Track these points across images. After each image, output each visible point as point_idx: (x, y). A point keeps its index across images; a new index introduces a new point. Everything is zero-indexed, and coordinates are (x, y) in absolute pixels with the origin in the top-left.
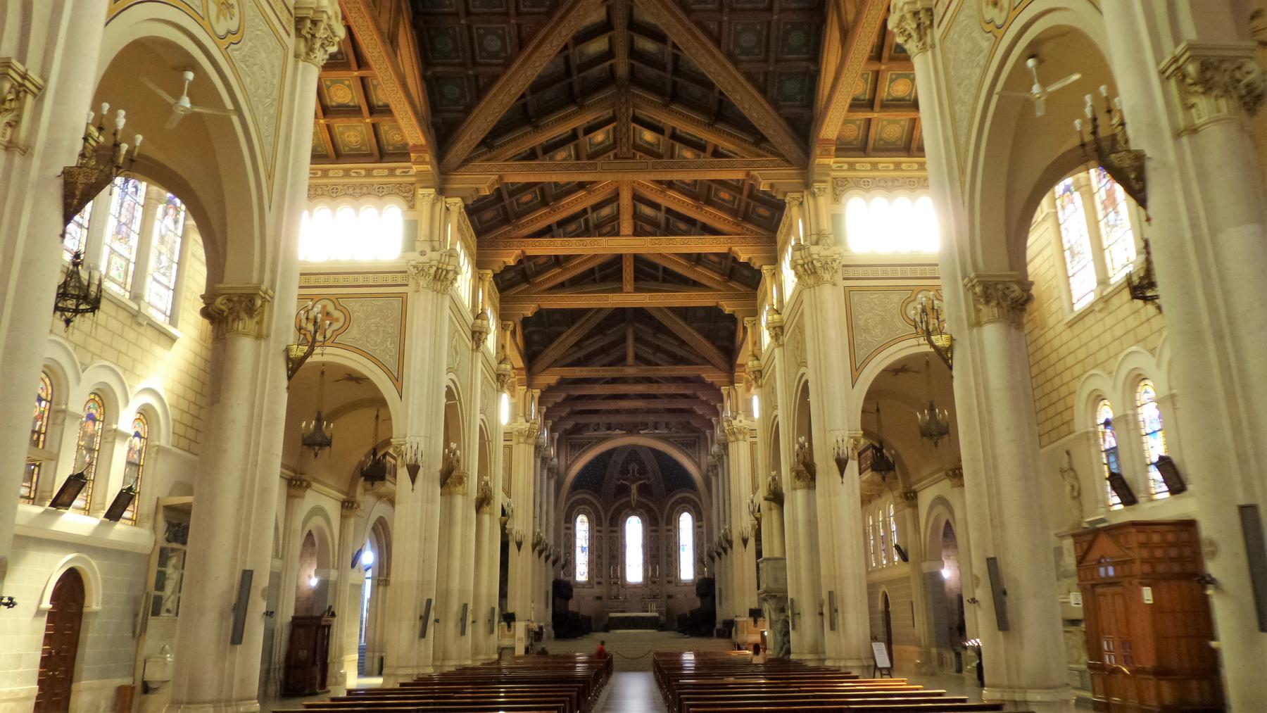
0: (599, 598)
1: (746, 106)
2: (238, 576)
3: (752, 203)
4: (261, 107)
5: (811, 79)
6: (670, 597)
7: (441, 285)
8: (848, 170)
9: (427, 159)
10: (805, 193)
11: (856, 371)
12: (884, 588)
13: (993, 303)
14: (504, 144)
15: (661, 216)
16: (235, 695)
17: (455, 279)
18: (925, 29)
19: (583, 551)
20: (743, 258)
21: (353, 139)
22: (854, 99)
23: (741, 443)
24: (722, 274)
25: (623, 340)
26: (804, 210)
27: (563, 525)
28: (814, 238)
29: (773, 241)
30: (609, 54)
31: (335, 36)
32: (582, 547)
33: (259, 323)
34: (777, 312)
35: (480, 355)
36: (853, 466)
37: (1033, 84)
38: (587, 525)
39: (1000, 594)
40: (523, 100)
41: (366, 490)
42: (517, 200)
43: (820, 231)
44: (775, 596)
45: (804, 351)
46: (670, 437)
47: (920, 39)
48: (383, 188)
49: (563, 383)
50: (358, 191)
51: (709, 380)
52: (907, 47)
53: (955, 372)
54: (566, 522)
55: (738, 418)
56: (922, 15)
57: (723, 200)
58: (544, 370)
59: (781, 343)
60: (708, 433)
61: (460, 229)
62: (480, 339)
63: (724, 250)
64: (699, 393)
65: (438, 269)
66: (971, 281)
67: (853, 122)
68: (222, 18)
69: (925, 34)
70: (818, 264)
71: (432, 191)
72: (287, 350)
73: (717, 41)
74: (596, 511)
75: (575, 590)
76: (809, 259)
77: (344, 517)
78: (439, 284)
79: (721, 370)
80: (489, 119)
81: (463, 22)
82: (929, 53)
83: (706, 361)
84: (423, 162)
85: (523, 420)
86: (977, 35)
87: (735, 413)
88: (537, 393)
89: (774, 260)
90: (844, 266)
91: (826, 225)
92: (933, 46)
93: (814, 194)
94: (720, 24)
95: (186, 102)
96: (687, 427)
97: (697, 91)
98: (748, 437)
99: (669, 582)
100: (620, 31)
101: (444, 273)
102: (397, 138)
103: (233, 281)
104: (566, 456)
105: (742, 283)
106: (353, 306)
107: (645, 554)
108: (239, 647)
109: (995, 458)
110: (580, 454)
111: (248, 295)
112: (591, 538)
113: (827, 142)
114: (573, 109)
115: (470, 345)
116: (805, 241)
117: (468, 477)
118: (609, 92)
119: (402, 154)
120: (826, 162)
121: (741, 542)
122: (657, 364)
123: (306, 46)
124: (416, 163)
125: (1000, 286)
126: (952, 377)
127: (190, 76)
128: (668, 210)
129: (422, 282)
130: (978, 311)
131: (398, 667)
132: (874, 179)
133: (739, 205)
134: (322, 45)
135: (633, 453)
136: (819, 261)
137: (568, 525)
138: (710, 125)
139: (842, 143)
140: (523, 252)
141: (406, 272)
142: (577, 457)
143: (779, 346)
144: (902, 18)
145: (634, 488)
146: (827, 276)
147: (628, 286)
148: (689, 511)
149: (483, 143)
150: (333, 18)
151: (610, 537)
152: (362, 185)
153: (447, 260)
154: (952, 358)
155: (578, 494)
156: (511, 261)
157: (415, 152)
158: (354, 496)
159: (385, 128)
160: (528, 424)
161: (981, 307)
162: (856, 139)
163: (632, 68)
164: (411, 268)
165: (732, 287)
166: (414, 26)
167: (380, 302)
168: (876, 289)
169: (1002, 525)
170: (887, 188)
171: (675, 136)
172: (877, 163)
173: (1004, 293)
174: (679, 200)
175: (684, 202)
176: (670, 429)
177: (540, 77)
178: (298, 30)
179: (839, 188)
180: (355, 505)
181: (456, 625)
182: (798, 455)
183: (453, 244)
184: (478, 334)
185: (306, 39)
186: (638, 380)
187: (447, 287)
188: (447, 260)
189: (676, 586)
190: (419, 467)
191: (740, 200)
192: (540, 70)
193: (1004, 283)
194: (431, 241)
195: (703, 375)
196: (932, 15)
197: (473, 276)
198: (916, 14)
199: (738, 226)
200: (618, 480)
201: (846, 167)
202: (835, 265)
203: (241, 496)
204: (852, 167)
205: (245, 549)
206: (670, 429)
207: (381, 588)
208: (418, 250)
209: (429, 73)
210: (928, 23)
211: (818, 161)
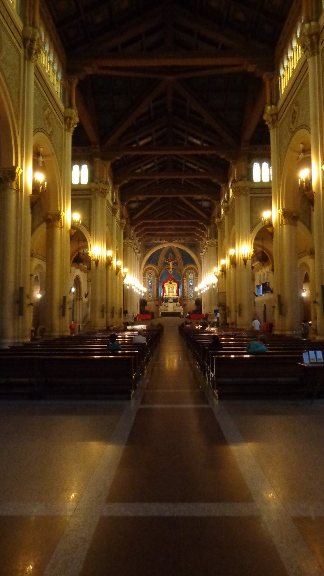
33: (61, 223)
34: (227, 202)
52: (269, 126)
54: (144, 276)
75: (147, 302)
89: (226, 182)
99: (185, 300)
110: (149, 250)
115: (112, 214)
134: (73, 126)
135: (170, 250)
137: (145, 278)
145: (171, 263)
164: (93, 189)
200: (165, 260)
210: (275, 119)
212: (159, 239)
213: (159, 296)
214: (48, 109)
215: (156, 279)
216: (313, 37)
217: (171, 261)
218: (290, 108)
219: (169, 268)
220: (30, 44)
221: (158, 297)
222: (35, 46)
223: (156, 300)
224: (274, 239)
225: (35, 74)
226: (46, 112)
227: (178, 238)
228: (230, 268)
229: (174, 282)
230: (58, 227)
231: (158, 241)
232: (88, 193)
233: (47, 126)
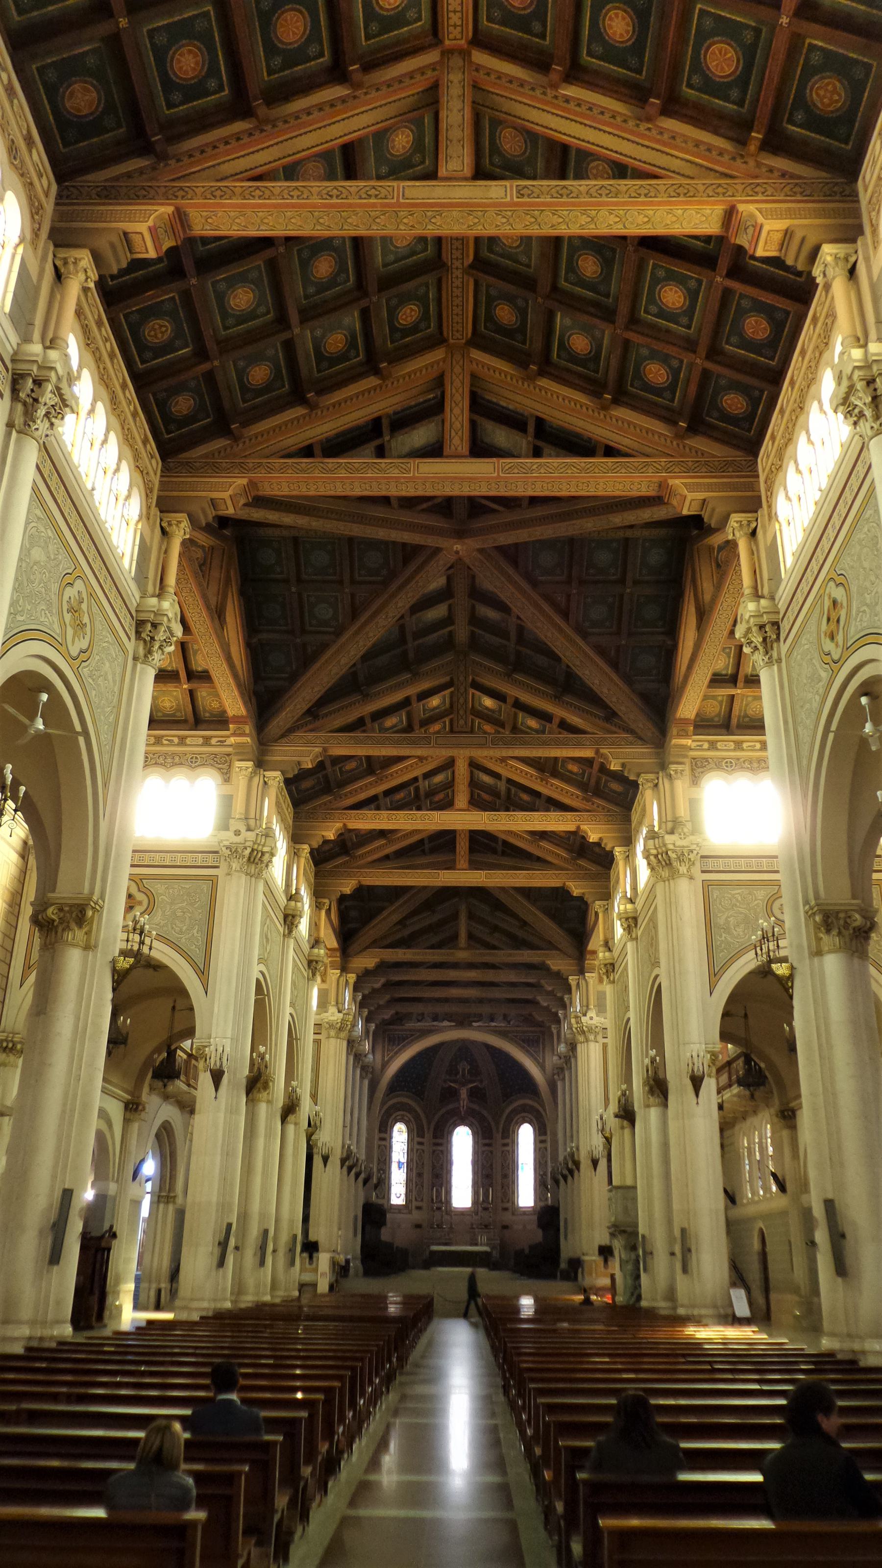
0: (418, 1226)
1: (597, 682)
2: (58, 1194)
3: (604, 778)
4: (102, 717)
5: (670, 653)
6: (505, 1227)
7: (256, 868)
9: (247, 731)
10: (661, 774)
11: (714, 976)
12: (761, 1224)
13: (835, 932)
14: (330, 713)
15: (502, 786)
16: (50, 1316)
17: (270, 861)
18: (772, 642)
19: (400, 1168)
20: (593, 838)
21: (167, 704)
22: (714, 674)
23: (592, 1045)
24: (570, 850)
25: (455, 916)
26: (658, 791)
27: (377, 1136)
28: (670, 825)
29: (627, 820)
30: (449, 620)
31: (173, 636)
32: (399, 1162)
34: (631, 901)
35: (292, 941)
36: (710, 1085)
37: (867, 721)
38: (405, 1136)
39: (838, 1237)
40: (354, 669)
41: (152, 1089)
42: (340, 769)
43: (677, 818)
44: (624, 1232)
45: (657, 950)
47: (767, 653)
48: (196, 758)
49: (383, 967)
50: (169, 760)
53: (796, 1002)
54: (380, 1131)
55: (589, 1014)
57: (571, 772)
58: (361, 952)
59: (634, 936)
61: (278, 804)
62: (292, 924)
63: (571, 828)
64: (543, 982)
65: (253, 850)
66: (811, 908)
67: (714, 697)
68: (76, 639)
69: (772, 648)
70: (673, 855)
71: (250, 764)
72: (114, 962)
73: (565, 614)
74: (417, 1118)
75: (388, 1216)
77: (127, 1121)
78: (253, 866)
80: (316, 689)
81: (294, 589)
82: (775, 667)
83: (551, 946)
84: (243, 734)
85: (333, 1010)
86: (817, 662)
88: (352, 978)
89: (628, 841)
90: (702, 857)
91: (682, 811)
92: (779, 661)
93: (670, 776)
94: (569, 596)
95: (40, 725)
96: (529, 1020)
97: (542, 660)
99: (506, 1209)
100: (461, 600)
101: (260, 855)
102: (215, 705)
103: (65, 890)
104: (383, 1052)
105: (594, 862)
106: (158, 888)
107: (475, 1173)
108: (55, 1268)
109: (834, 1094)
110: (400, 1050)
111: (79, 905)
112: (410, 1151)
113: (685, 721)
114: (407, 676)
115: (281, 930)
116: (660, 828)
117: (273, 1082)
118: (449, 657)
119: (220, 721)
121: (590, 1162)
122: (494, 948)
123: (144, 649)
124: (234, 734)
125: (842, 915)
126: (792, 1007)
127: (44, 697)
128: (509, 781)
129: (235, 865)
130: (819, 940)
131: (192, 1300)
132: (738, 759)
133: (589, 779)
135: (464, 1049)
136: (674, 851)
137: (383, 1135)
139: (703, 720)
141: (217, 852)
142: (396, 1053)
143: (632, 939)
144: (749, 630)
145: (464, 1093)
146: (683, 869)
147: (462, 862)
149: (309, 712)
150: (173, 621)
151: (434, 1151)
152: (173, 755)
153: (263, 841)
154: (792, 987)
155: (397, 1096)
156: (331, 835)
157: (234, 723)
158: (139, 1097)
159: (203, 693)
160: (341, 1015)
161: (822, 935)
162: (719, 715)
164: (224, 849)
165: (580, 866)
166: (242, 593)
167: (187, 885)
168: (739, 884)
169: (842, 1165)
170: (751, 769)
171: (519, 705)
172: (743, 742)
173: (846, 922)
174: (522, 771)
176: (509, 1022)
177: (374, 645)
178: (138, 633)
180: (140, 1108)
181: (255, 1254)
182: (647, 1071)
183: (269, 822)
184: (290, 918)
185: (145, 641)
187: (261, 871)
188: (263, 841)
189: (513, 1214)
190: (224, 1072)
191: (590, 774)
192: (373, 640)
193: (846, 911)
194: (246, 819)
195: (548, 962)
196: (779, 628)
197: (288, 852)
198: (762, 627)
199: (588, 801)
200: (445, 1081)
201: (706, 746)
202: (692, 856)
203: (63, 1112)
204: (713, 746)
205: (65, 1166)
206: (509, 1022)
207: (162, 1206)
208: (233, 828)
209: (255, 640)
211: (674, 741)
214: (79, 585)
215: (417, 1139)
218: (820, 597)
220: (32, 391)
222: (48, 397)
225: (38, 467)
226: (70, 592)
230: (75, 946)
232: (210, 860)
233: (70, 632)
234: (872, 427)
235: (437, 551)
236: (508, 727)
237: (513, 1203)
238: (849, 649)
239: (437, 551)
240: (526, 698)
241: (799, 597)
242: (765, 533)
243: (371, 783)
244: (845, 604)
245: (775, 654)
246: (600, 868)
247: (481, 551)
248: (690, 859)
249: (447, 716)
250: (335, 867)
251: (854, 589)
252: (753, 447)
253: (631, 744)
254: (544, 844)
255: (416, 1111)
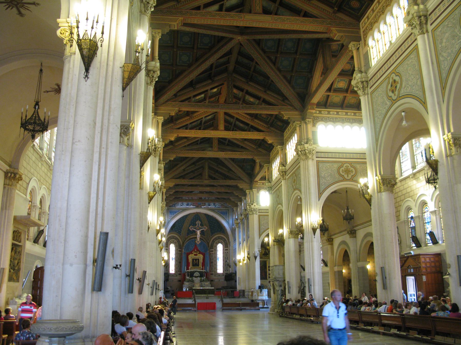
8: (319, 114)
10: (302, 122)
13: (386, 185)
18: (365, 88)
23: (255, 215)
25: (203, 167)
28: (306, 140)
36: (318, 231)
44: (278, 280)
46: (216, 210)
51: (241, 187)
52: (358, 92)
56: (364, 83)
59: (285, 178)
60: (235, 209)
69: (365, 90)
70: (307, 152)
75: (170, 277)
76: (304, 149)
79: (246, 183)
82: (366, 96)
83: (240, 179)
87: (252, 202)
90: (317, 152)
91: (310, 136)
92: (368, 94)
93: (306, 123)
98: (257, 213)
99: (212, 274)
113: (313, 104)
118: (224, 75)
120: (313, 112)
121: (254, 258)
122: (217, 179)
132: (329, 118)
138: (265, 92)
140: (178, 135)
143: (284, 179)
144: (358, 83)
145: (198, 232)
146: (310, 156)
148: (221, 243)
162: (323, 101)
163: (235, 67)
170: (333, 122)
175: (246, 117)
179: (315, 121)
186: (207, 186)
193: (389, 179)
195: (239, 185)
196: (368, 83)
198: (362, 82)
199: (268, 128)
202: (313, 152)
204: (320, 112)
206: (216, 206)
210: (366, 86)
211: (309, 111)
212: (185, 203)
213: (220, 269)
215: (179, 249)
216: (422, 18)
217: (199, 230)
218: (388, 77)
219: (196, 238)
221: (181, 271)
223: (179, 274)
224: (372, 207)
227: (207, 204)
228: (290, 238)
229: (199, 254)
231: (185, 206)
234: (419, 32)
235: (231, 39)
236: (242, 100)
237: (215, 272)
238: (400, 98)
239: (231, 39)
240: (251, 90)
241: (378, 75)
242: (363, 49)
243: (187, 119)
244: (399, 82)
245: (366, 92)
246: (267, 152)
247: (248, 40)
248: (313, 153)
249: (217, 95)
250: (167, 150)
251: (404, 79)
252: (359, 18)
253: (292, 110)
254: (246, 142)
255: (179, 240)
